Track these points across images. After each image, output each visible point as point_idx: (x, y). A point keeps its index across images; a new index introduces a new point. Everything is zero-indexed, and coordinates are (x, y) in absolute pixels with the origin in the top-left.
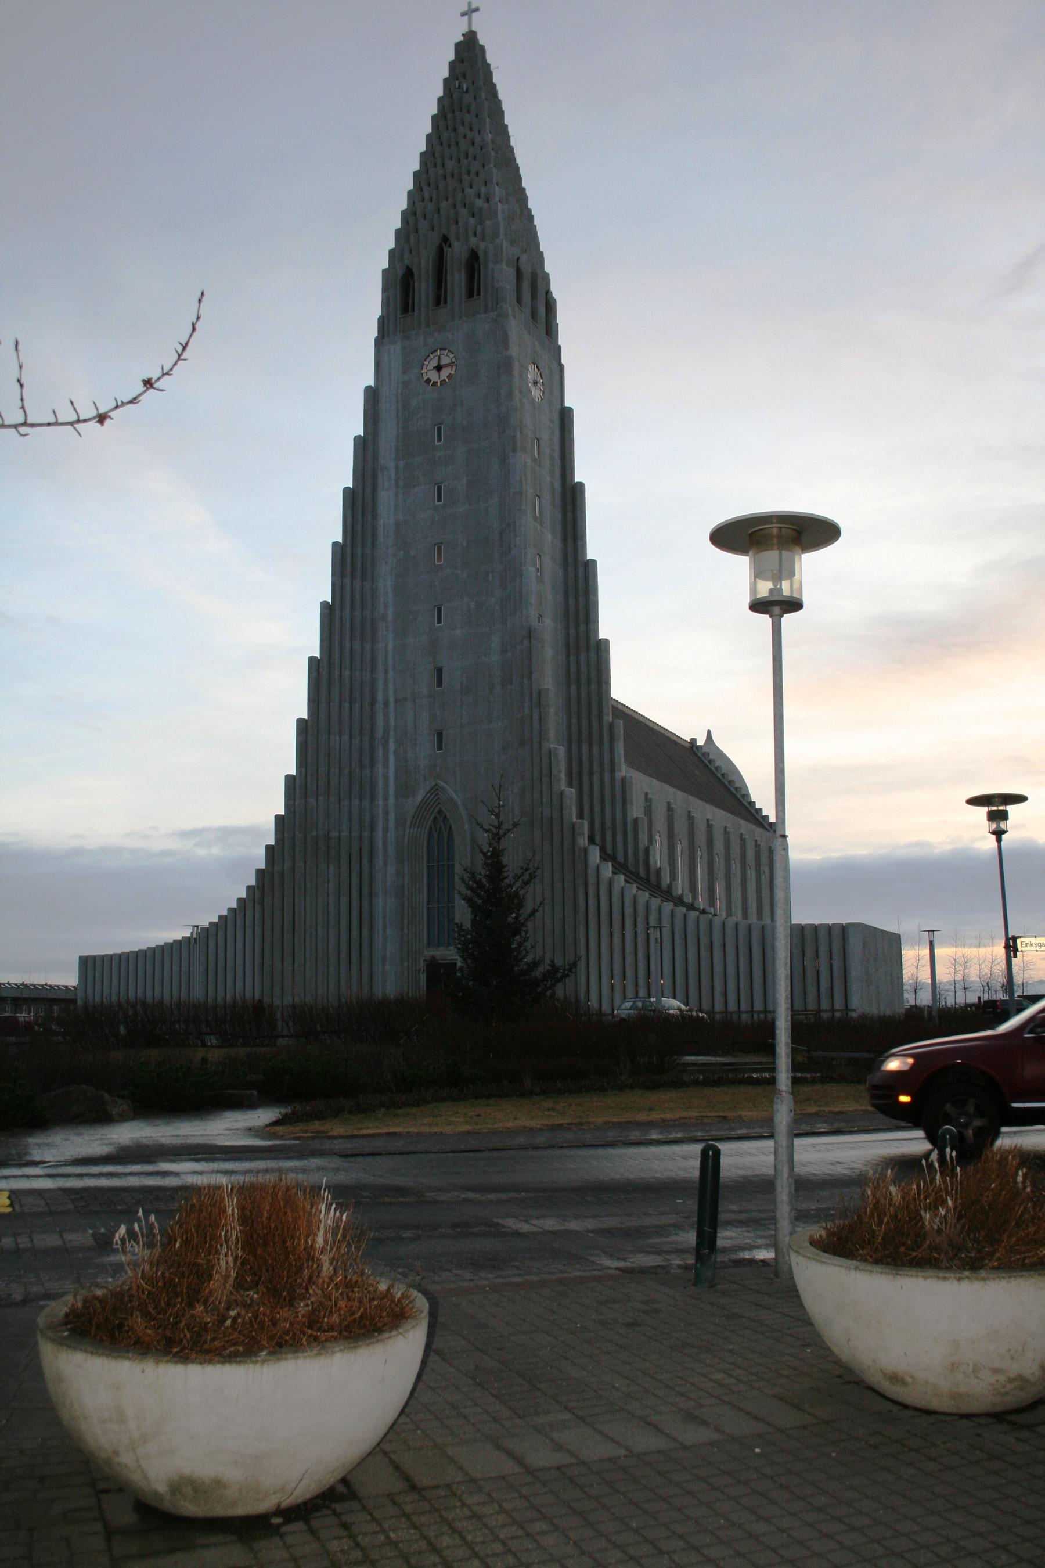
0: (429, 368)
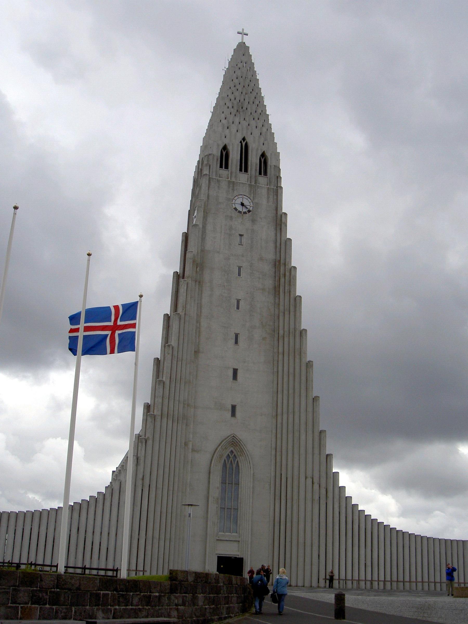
0: (236, 202)
